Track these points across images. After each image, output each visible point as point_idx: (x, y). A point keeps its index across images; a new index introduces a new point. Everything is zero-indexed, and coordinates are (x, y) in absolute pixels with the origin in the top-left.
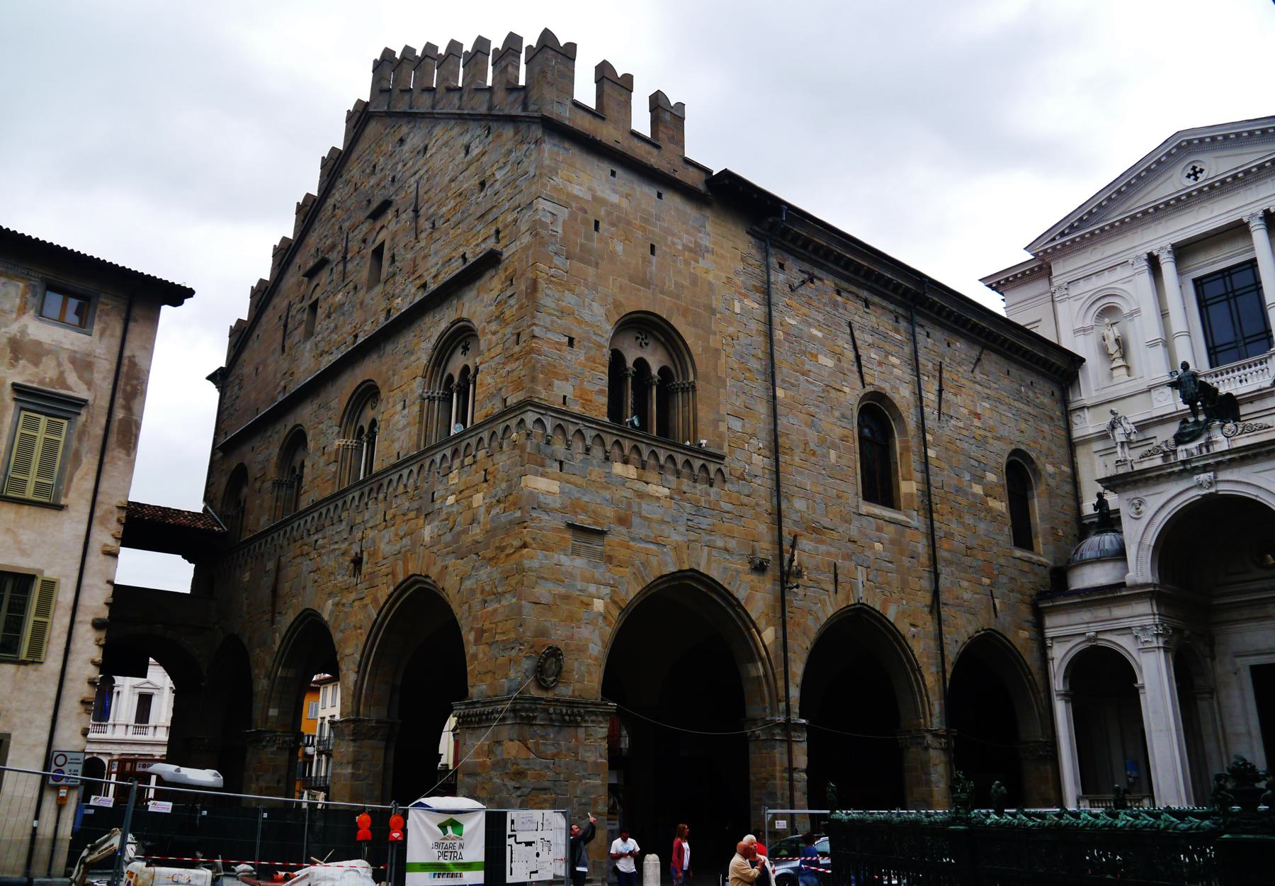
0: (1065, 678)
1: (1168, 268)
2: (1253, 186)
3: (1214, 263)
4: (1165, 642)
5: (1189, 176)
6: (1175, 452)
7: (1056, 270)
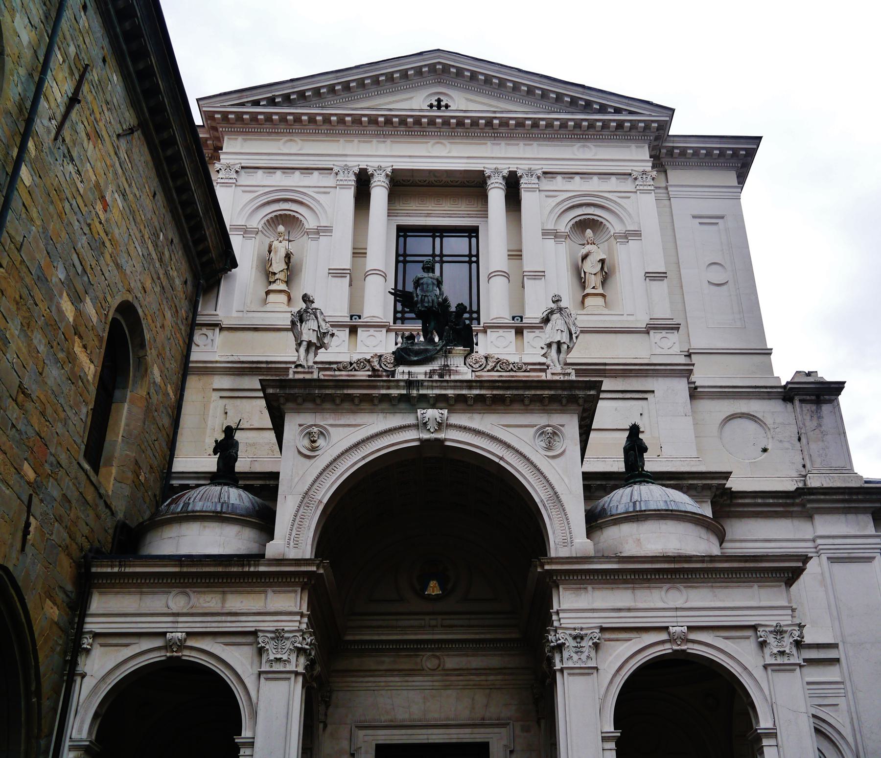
1: (379, 195)
2: (503, 143)
6: (393, 373)
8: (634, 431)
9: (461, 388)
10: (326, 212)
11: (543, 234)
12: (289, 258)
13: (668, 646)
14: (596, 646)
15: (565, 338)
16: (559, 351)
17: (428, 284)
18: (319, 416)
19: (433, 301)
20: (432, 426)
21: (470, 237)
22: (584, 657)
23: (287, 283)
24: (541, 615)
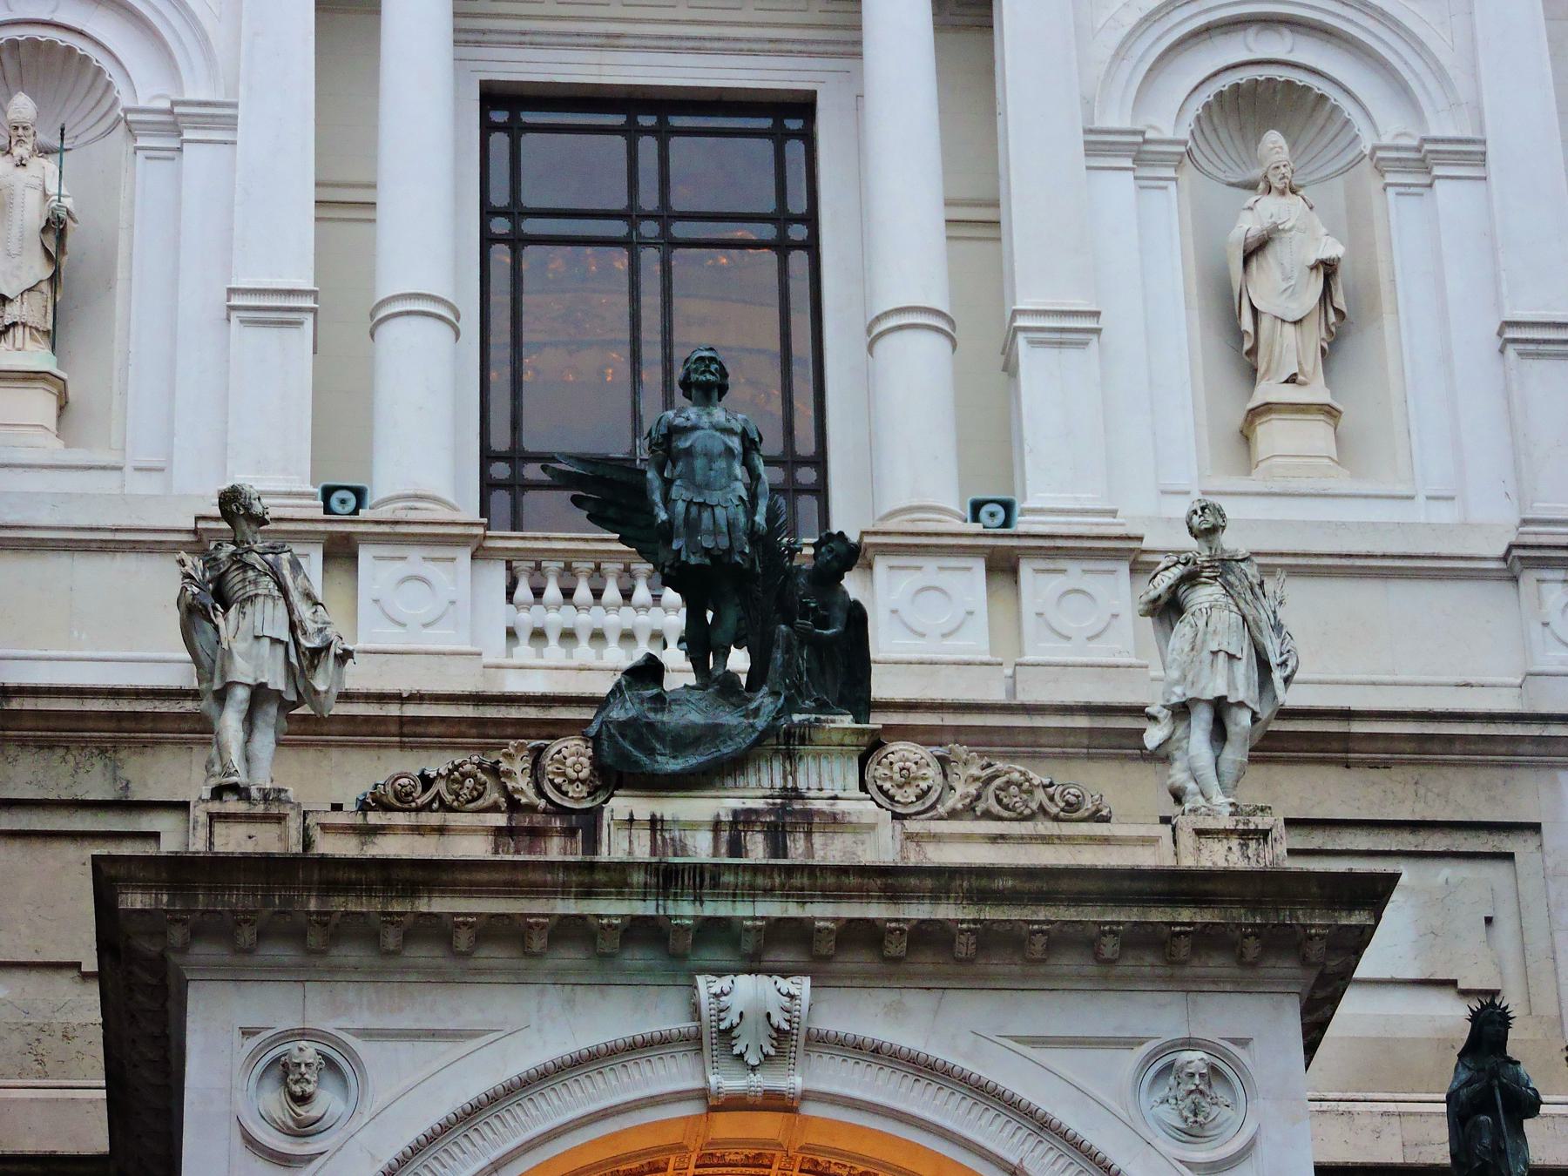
3: (611, 42)
6: (587, 825)
8: (1489, 1026)
9: (863, 895)
10: (204, 40)
11: (1092, 149)
12: (61, 236)
16: (1219, 733)
17: (710, 457)
18: (316, 995)
19: (731, 525)
20: (750, 1043)
21: (779, 137)
23: (52, 337)
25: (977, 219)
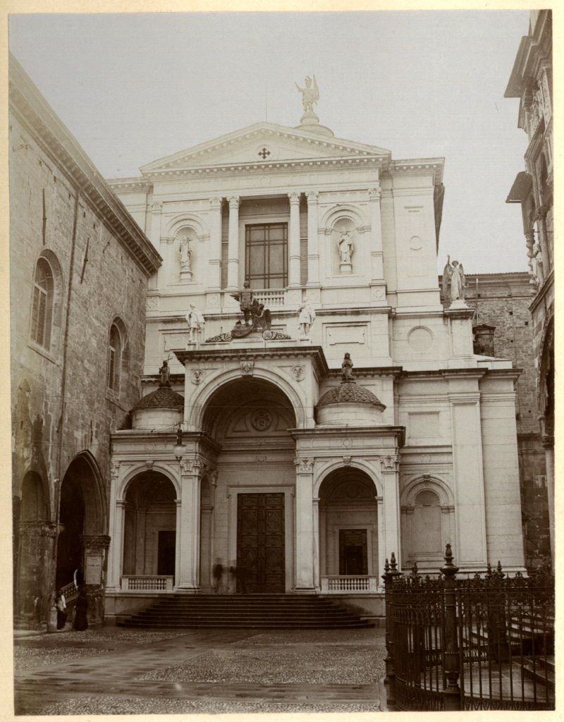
0: (125, 491)
1: (234, 212)
4: (200, 473)
5: (260, 154)
7: (156, 190)
13: (342, 464)
14: (313, 465)
15: (308, 321)
21: (284, 228)
22: (307, 469)
24: (292, 450)
25: (304, 241)
